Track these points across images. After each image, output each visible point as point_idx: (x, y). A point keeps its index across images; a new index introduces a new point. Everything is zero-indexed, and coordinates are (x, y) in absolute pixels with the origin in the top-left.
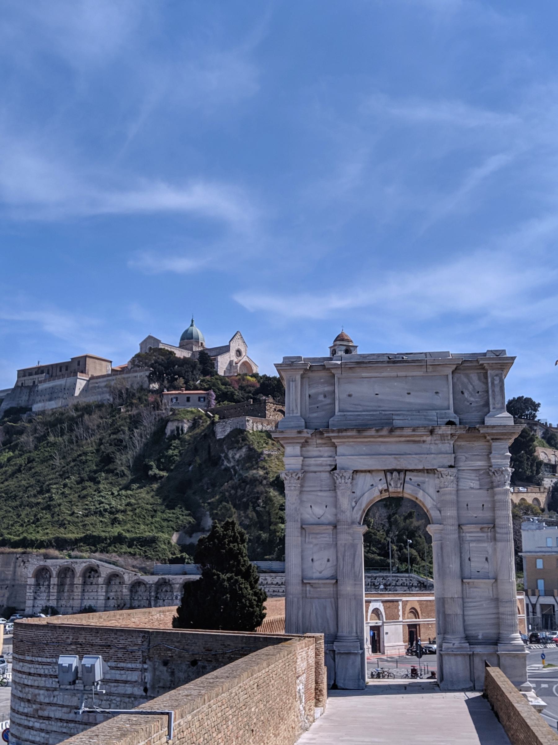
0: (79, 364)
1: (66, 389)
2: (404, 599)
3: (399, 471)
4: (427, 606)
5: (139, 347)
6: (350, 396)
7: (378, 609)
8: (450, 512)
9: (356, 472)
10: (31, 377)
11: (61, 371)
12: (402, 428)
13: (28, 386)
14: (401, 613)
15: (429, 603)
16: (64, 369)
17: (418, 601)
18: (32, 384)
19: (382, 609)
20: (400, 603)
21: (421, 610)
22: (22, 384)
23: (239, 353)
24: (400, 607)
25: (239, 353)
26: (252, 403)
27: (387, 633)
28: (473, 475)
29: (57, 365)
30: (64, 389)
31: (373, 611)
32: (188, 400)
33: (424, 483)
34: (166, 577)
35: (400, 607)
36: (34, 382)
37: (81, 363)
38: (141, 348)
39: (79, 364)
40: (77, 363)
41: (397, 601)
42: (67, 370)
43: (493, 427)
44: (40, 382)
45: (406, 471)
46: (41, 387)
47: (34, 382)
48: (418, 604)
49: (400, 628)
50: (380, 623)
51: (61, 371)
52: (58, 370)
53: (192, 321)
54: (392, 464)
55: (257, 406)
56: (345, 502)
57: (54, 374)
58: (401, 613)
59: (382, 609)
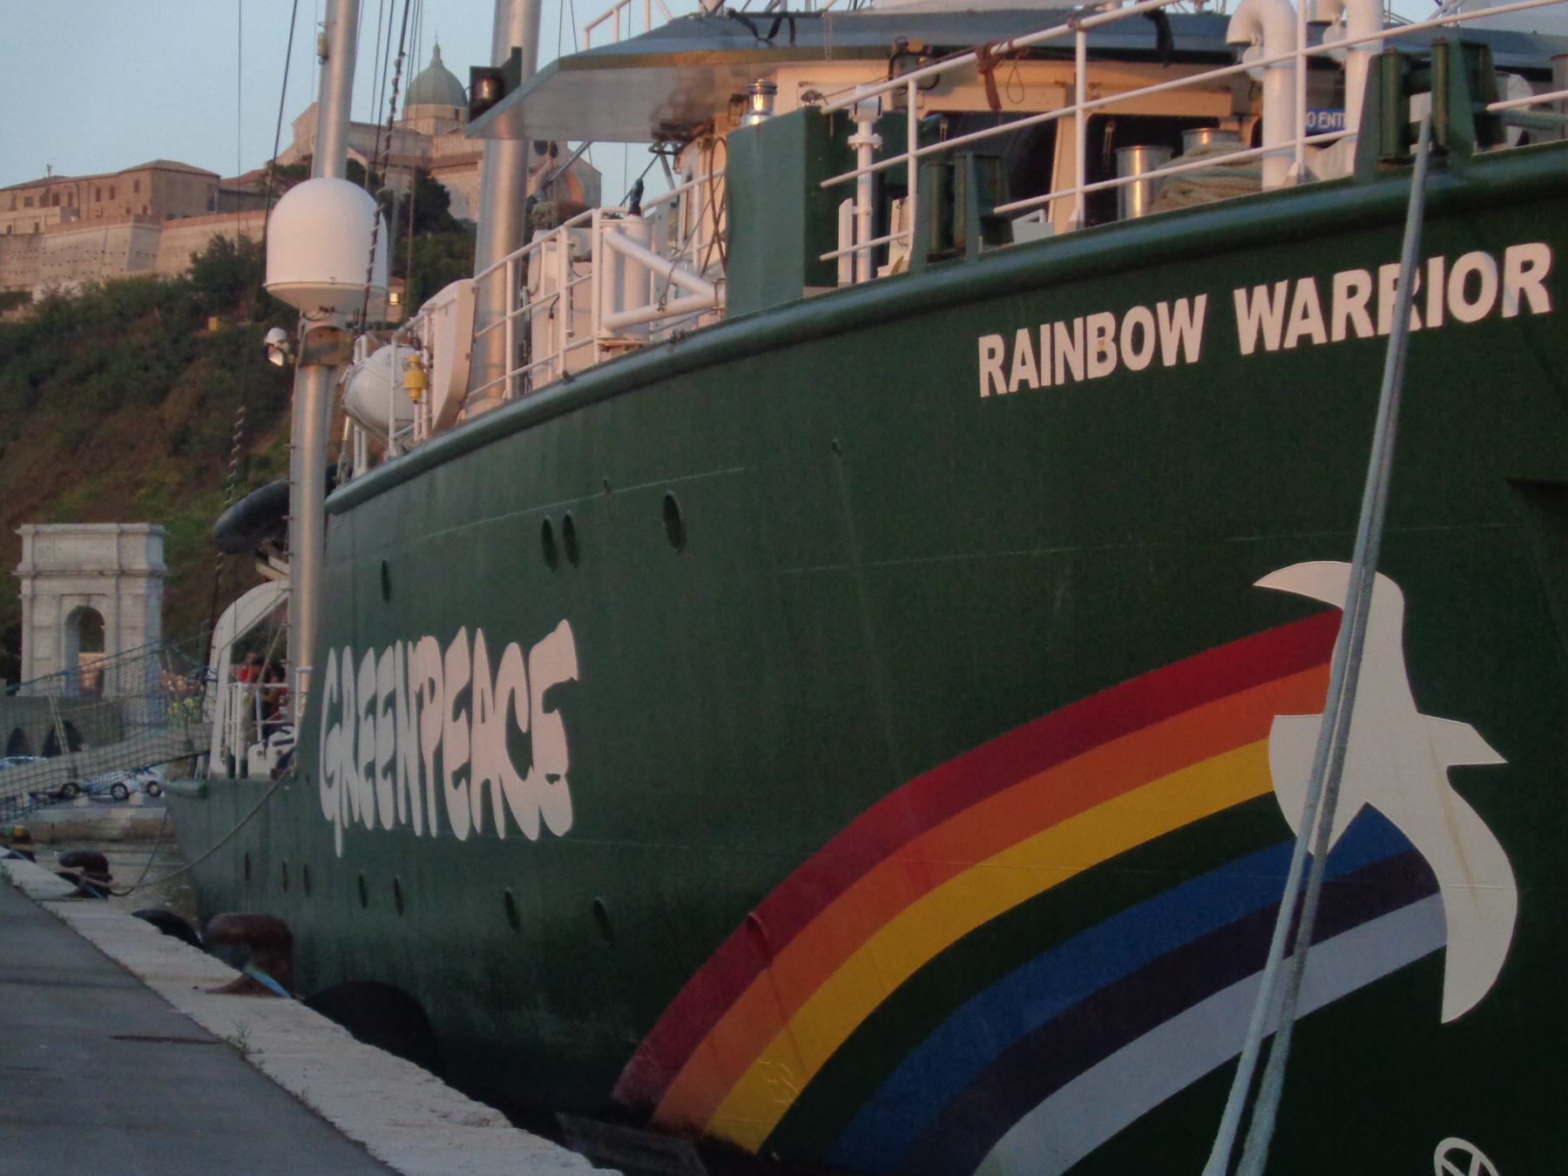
1: (108, 251)
9: (63, 595)
10: (30, 212)
11: (98, 198)
12: (85, 571)
13: (22, 235)
16: (105, 195)
18: (31, 231)
22: (9, 228)
29: (89, 180)
30: (103, 252)
36: (37, 226)
37: (142, 187)
40: (131, 184)
42: (112, 197)
43: (135, 570)
44: (50, 228)
46: (53, 242)
47: (37, 226)
51: (98, 198)
52: (93, 196)
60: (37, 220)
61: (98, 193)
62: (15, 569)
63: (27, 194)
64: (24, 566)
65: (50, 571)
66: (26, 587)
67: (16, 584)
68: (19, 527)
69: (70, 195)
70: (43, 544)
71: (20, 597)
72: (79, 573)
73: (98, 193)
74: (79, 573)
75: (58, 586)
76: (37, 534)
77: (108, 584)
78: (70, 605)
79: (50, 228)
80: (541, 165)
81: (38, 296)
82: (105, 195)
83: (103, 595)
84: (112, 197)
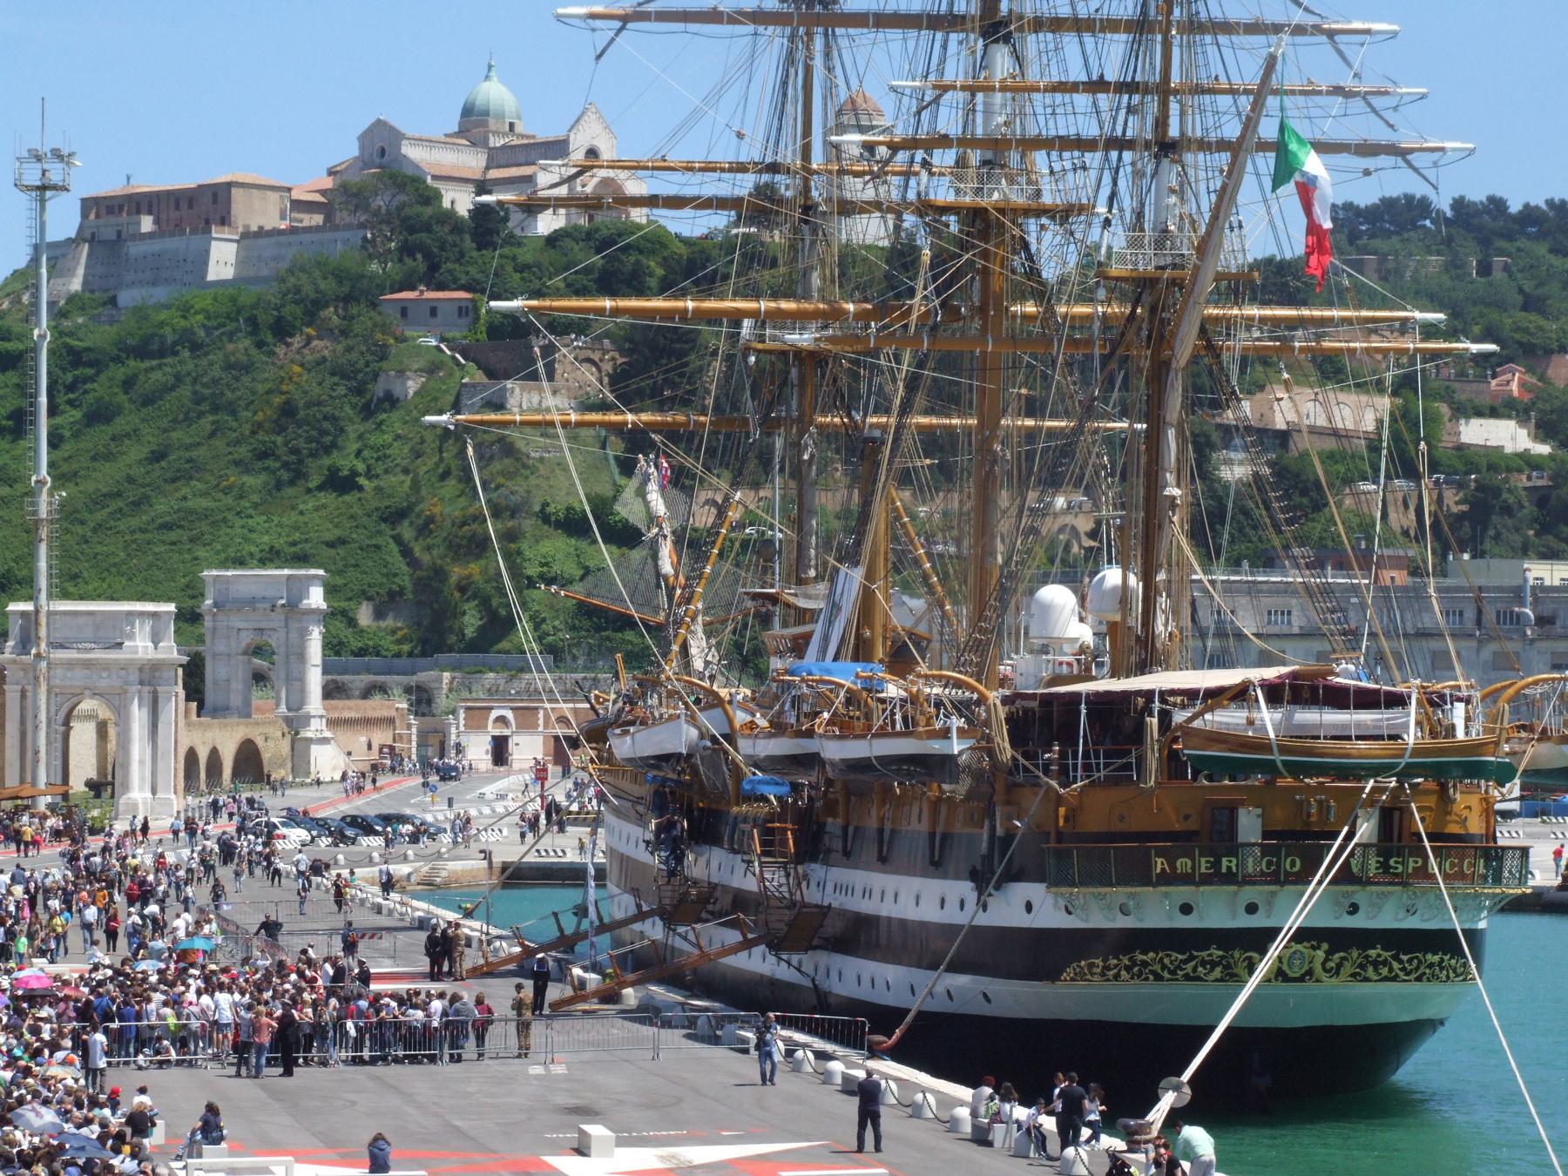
5: (356, 144)
8: (282, 649)
11: (177, 208)
13: (106, 242)
16: (184, 204)
29: (169, 193)
32: (433, 312)
34: (339, 678)
36: (119, 233)
38: (362, 148)
41: (536, 709)
42: (191, 206)
49: (540, 739)
50: (506, 732)
51: (177, 208)
53: (490, 67)
54: (257, 626)
56: (233, 644)
59: (509, 715)
84: (191, 206)
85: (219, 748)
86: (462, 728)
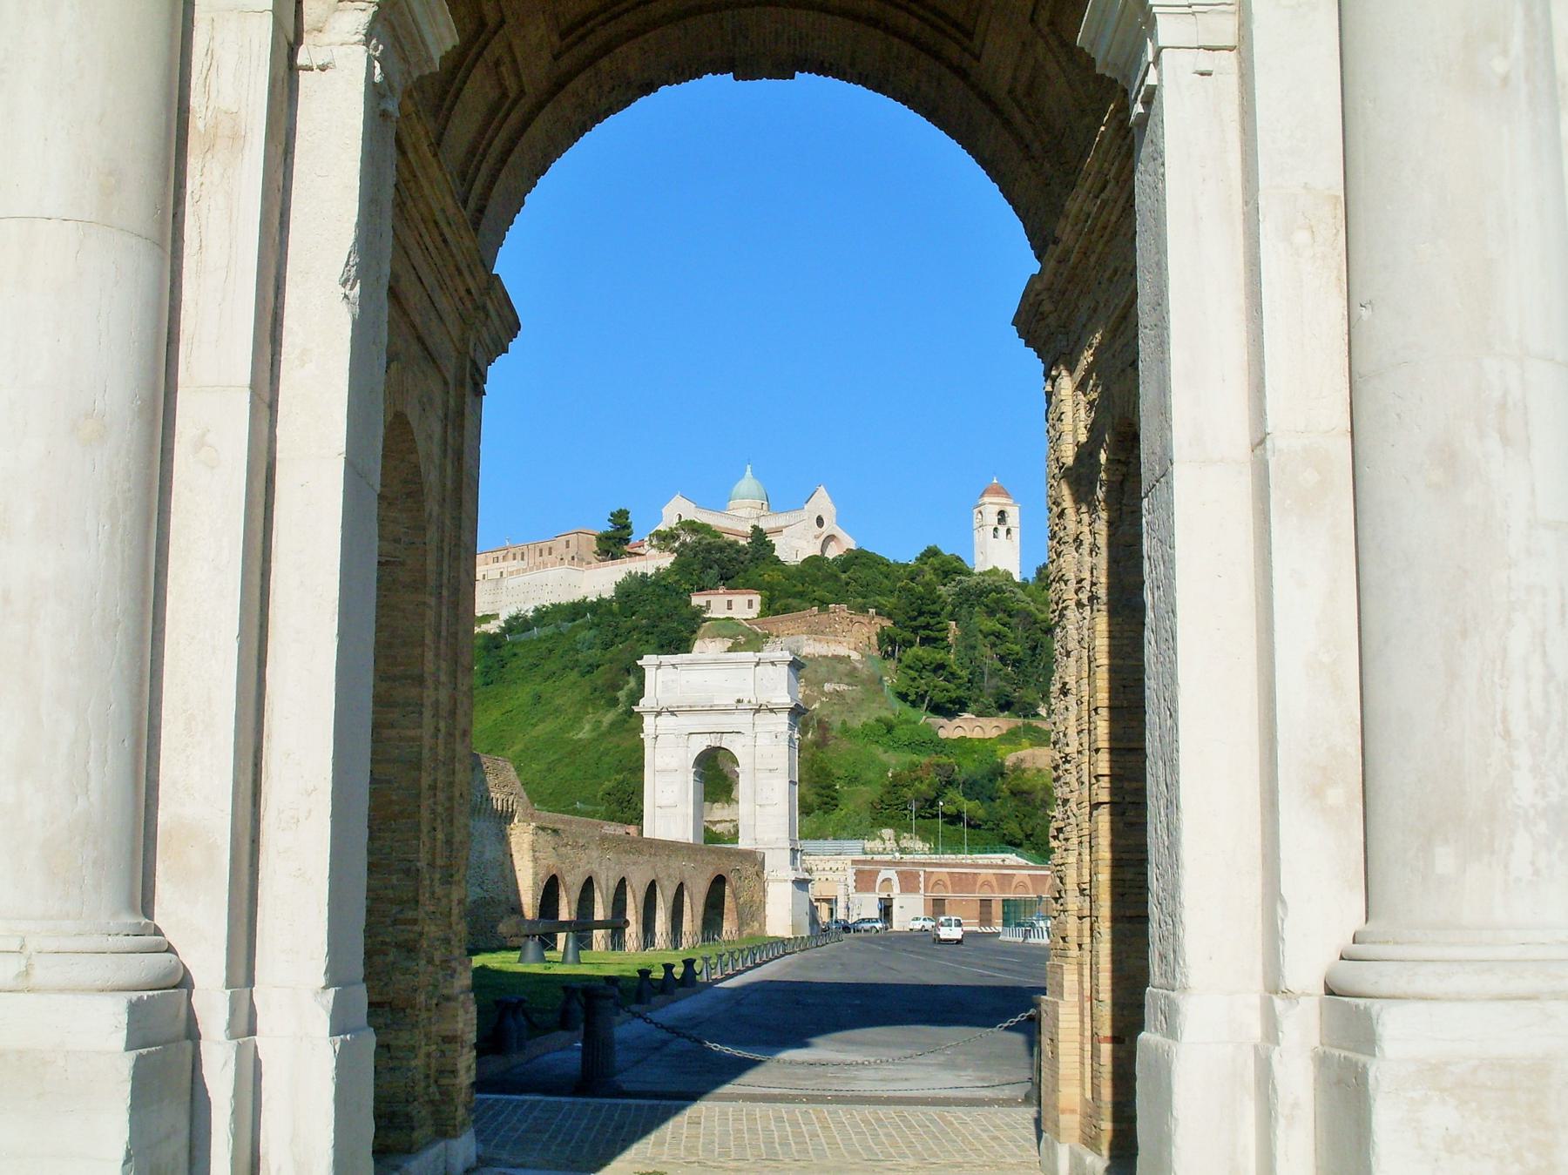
0: (568, 547)
2: (927, 869)
3: (718, 733)
4: (960, 879)
6: (688, 682)
7: (890, 879)
11: (541, 555)
14: (922, 885)
15: (964, 876)
16: (545, 552)
17: (948, 873)
18: (499, 577)
19: (895, 879)
20: (922, 873)
21: (952, 883)
22: (484, 575)
23: (820, 521)
24: (922, 879)
25: (820, 521)
26: (816, 613)
27: (901, 907)
28: (767, 735)
31: (883, 881)
33: (734, 741)
35: (922, 879)
36: (502, 573)
39: (568, 547)
42: (550, 554)
43: (776, 704)
44: (511, 573)
45: (723, 733)
47: (502, 573)
48: (947, 876)
51: (541, 555)
52: (538, 553)
55: (824, 616)
57: (531, 561)
58: (922, 885)
60: (502, 570)
61: (541, 551)
62: (638, 705)
63: (495, 555)
64: (645, 704)
65: (678, 707)
66: (648, 721)
67: (640, 717)
68: (641, 658)
69: (523, 553)
70: (665, 675)
71: (642, 736)
72: (711, 710)
73: (541, 551)
74: (711, 710)
75: (686, 722)
76: (659, 666)
77: (742, 720)
78: (700, 745)
79: (511, 573)
80: (821, 535)
81: (504, 616)
82: (545, 552)
83: (740, 732)
84: (550, 554)
85: (688, 883)
86: (854, 891)
